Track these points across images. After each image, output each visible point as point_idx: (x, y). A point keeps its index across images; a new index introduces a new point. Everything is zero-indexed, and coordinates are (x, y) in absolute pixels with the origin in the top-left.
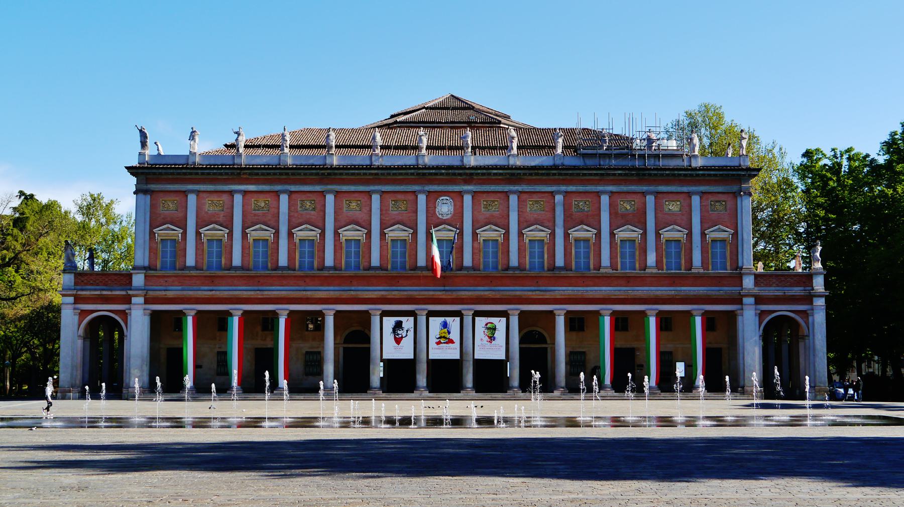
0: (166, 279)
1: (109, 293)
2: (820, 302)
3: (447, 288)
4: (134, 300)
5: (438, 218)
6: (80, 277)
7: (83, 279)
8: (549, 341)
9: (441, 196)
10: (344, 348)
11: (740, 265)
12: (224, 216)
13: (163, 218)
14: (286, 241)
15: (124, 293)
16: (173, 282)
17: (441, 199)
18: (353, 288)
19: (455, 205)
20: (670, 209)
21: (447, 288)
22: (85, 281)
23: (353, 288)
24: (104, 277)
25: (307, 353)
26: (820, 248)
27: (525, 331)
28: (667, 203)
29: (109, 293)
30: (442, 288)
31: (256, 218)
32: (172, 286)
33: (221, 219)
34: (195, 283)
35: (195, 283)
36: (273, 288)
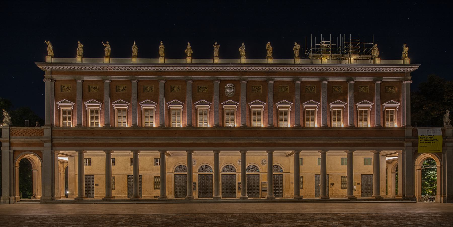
1: (30, 140)
3: (232, 137)
4: (46, 144)
5: (227, 96)
9: (227, 83)
12: (99, 95)
15: (39, 140)
17: (228, 84)
18: (176, 138)
20: (362, 91)
21: (232, 137)
23: (176, 138)
26: (447, 115)
29: (30, 140)
30: (229, 137)
36: (129, 137)
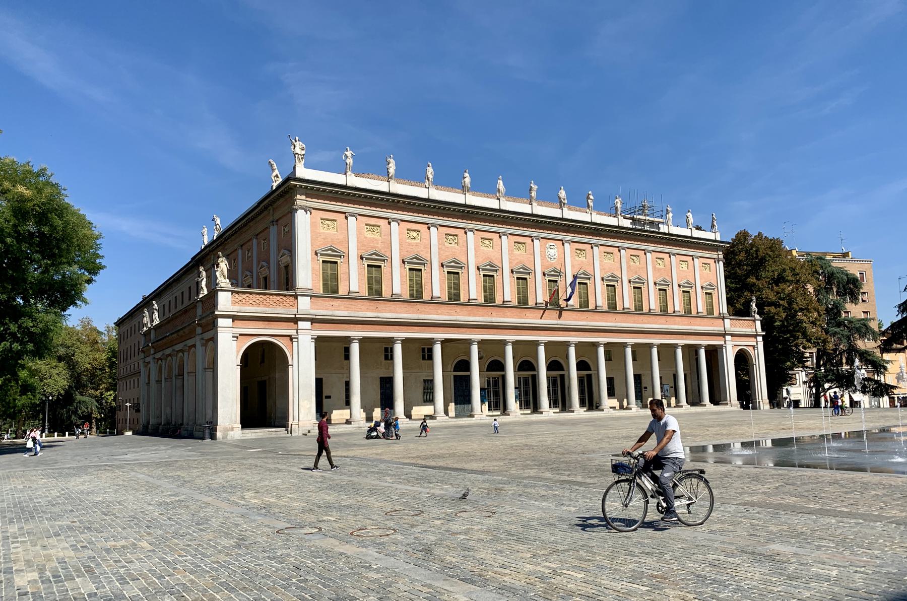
0: (332, 303)
2: (760, 339)
6: (237, 296)
7: (240, 298)
8: (592, 369)
10: (455, 376)
11: (721, 312)
13: (324, 239)
14: (438, 272)
16: (339, 306)
19: (558, 251)
22: (244, 301)
24: (265, 297)
25: (424, 381)
27: (578, 360)
28: (681, 263)
31: (411, 247)
32: (338, 310)
33: (379, 245)
34: (361, 309)
35: (361, 309)
